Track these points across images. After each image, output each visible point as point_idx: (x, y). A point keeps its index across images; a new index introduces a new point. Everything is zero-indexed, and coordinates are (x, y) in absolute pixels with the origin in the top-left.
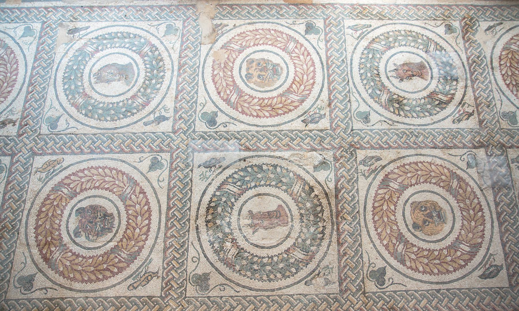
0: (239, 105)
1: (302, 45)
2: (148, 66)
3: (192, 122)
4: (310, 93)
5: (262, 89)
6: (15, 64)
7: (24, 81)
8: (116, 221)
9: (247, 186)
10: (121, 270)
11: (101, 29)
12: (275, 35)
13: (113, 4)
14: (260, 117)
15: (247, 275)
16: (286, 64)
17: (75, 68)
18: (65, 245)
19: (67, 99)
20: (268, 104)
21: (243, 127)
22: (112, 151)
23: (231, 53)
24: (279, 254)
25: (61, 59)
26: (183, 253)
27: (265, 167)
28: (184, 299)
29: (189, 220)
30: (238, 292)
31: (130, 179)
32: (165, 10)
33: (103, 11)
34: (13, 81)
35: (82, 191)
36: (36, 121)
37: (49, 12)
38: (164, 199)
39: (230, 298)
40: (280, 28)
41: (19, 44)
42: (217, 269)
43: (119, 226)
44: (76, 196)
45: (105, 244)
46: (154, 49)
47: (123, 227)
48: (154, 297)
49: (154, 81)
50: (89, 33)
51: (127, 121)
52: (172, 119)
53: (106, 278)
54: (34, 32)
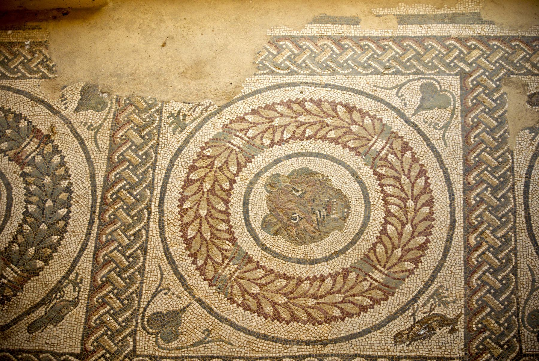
6: (419, 176)
34: (425, 219)
36: (506, 321)
41: (416, 126)
54: (447, 98)
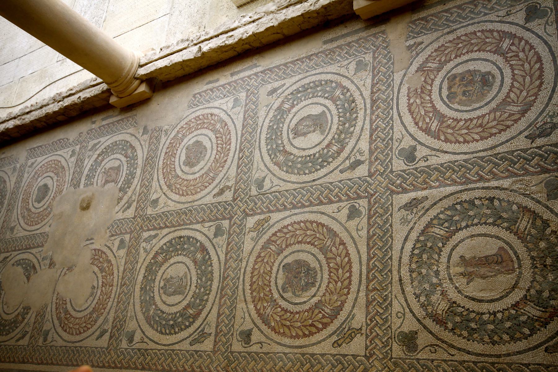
0: (441, 133)
1: (521, 39)
2: (340, 110)
3: (389, 162)
4: (536, 98)
5: (468, 108)
7: (236, 149)
8: (318, 275)
9: (457, 227)
10: (325, 325)
11: (295, 83)
12: (483, 37)
13: (304, 55)
14: (468, 142)
15: (462, 335)
16: (500, 69)
17: (275, 127)
18: (275, 300)
19: (270, 158)
20: (478, 125)
21: (447, 158)
22: (311, 204)
23: (428, 74)
24: (503, 310)
25: (264, 122)
26: (386, 307)
27: (477, 202)
28: (390, 360)
29: (391, 271)
30: (452, 355)
31: (330, 230)
32: (354, 46)
33: (295, 65)
35: (287, 246)
37: (251, 79)
38: (363, 249)
39: (443, 362)
40: (490, 26)
42: (425, 327)
43: (321, 280)
44: (282, 253)
45: (310, 299)
46: (345, 91)
47: (326, 281)
48: (358, 356)
49: (347, 125)
50: (285, 90)
51: (324, 171)
52: (367, 162)
53: (311, 334)
54: (241, 102)
